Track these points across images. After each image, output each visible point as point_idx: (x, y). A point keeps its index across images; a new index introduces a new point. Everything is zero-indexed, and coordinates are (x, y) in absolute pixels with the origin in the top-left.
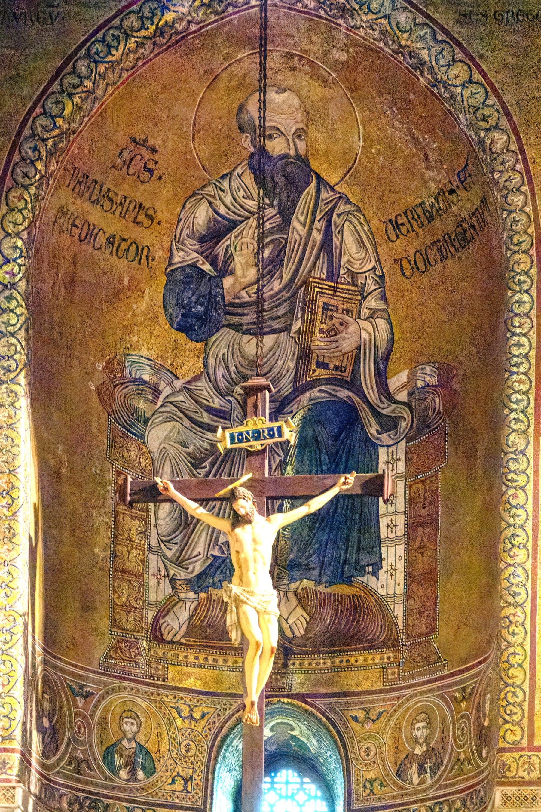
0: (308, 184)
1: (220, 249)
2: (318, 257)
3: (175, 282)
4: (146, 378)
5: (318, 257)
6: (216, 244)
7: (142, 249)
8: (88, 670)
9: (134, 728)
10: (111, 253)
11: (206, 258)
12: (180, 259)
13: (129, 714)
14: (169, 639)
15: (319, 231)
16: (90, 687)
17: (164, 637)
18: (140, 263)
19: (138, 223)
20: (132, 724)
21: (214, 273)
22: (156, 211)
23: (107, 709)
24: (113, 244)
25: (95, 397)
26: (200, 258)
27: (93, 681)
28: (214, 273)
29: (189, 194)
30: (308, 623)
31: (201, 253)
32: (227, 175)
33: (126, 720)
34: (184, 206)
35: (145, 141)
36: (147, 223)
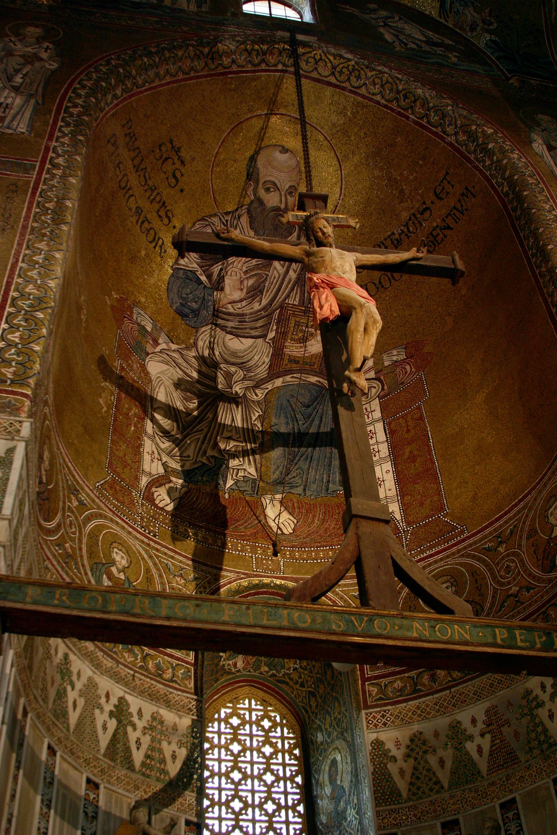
0: (291, 234)
1: (216, 269)
2: (292, 289)
3: (178, 278)
4: (149, 330)
5: (292, 289)
6: (213, 265)
7: (159, 239)
8: (84, 482)
9: (124, 562)
10: (137, 222)
11: (204, 271)
12: (184, 263)
13: (120, 547)
14: (161, 505)
15: (295, 271)
16: (83, 497)
17: (157, 502)
18: (155, 247)
19: (160, 217)
20: (122, 557)
21: (209, 286)
22: (173, 216)
23: (99, 529)
24: (140, 215)
25: (109, 309)
26: (199, 270)
27: (88, 495)
28: (209, 286)
29: (199, 218)
30: (295, 525)
31: (201, 267)
32: (230, 212)
33: (115, 550)
34: (194, 224)
35: (179, 149)
36: (166, 221)
